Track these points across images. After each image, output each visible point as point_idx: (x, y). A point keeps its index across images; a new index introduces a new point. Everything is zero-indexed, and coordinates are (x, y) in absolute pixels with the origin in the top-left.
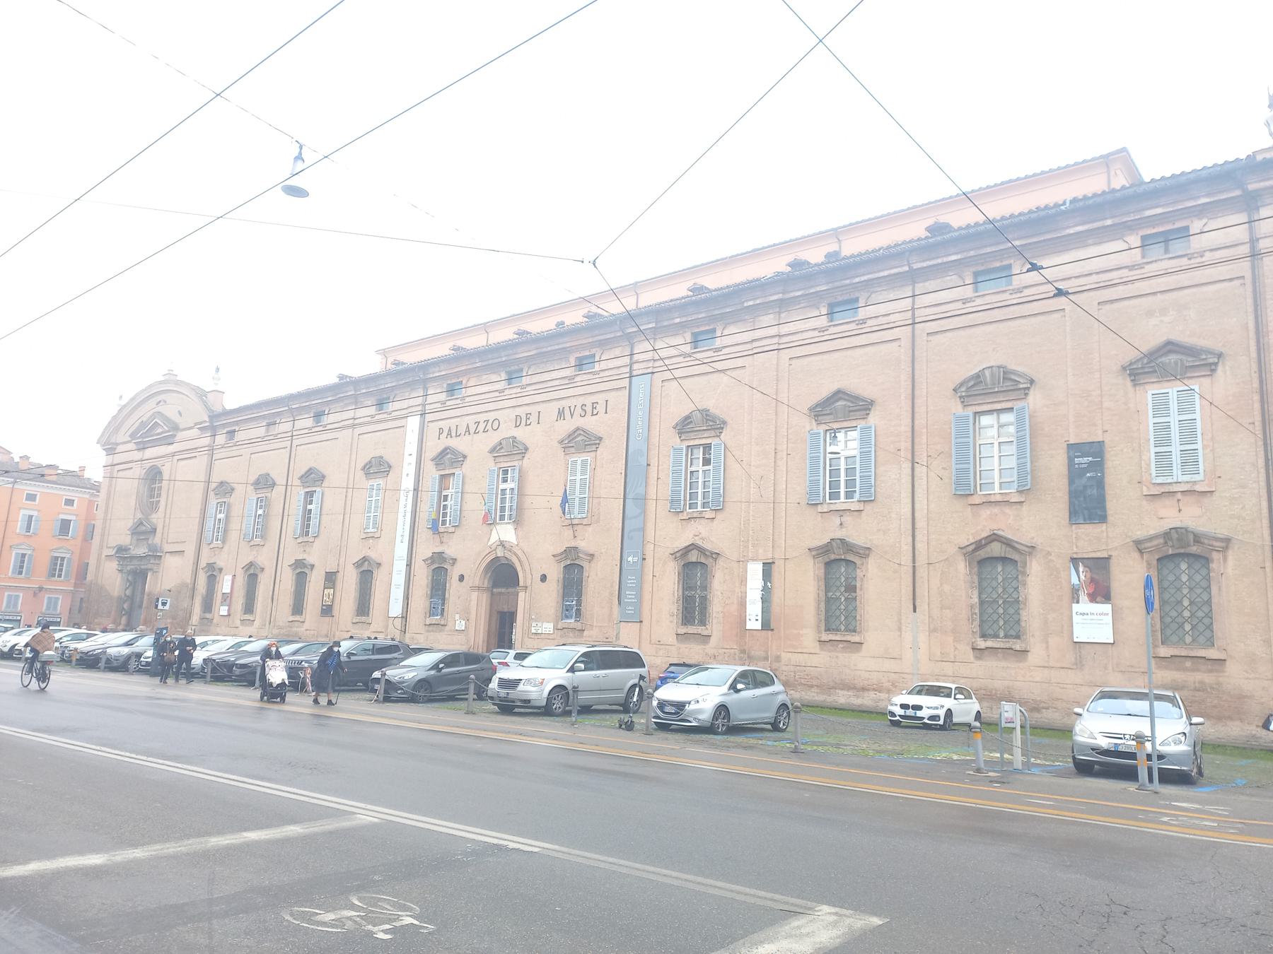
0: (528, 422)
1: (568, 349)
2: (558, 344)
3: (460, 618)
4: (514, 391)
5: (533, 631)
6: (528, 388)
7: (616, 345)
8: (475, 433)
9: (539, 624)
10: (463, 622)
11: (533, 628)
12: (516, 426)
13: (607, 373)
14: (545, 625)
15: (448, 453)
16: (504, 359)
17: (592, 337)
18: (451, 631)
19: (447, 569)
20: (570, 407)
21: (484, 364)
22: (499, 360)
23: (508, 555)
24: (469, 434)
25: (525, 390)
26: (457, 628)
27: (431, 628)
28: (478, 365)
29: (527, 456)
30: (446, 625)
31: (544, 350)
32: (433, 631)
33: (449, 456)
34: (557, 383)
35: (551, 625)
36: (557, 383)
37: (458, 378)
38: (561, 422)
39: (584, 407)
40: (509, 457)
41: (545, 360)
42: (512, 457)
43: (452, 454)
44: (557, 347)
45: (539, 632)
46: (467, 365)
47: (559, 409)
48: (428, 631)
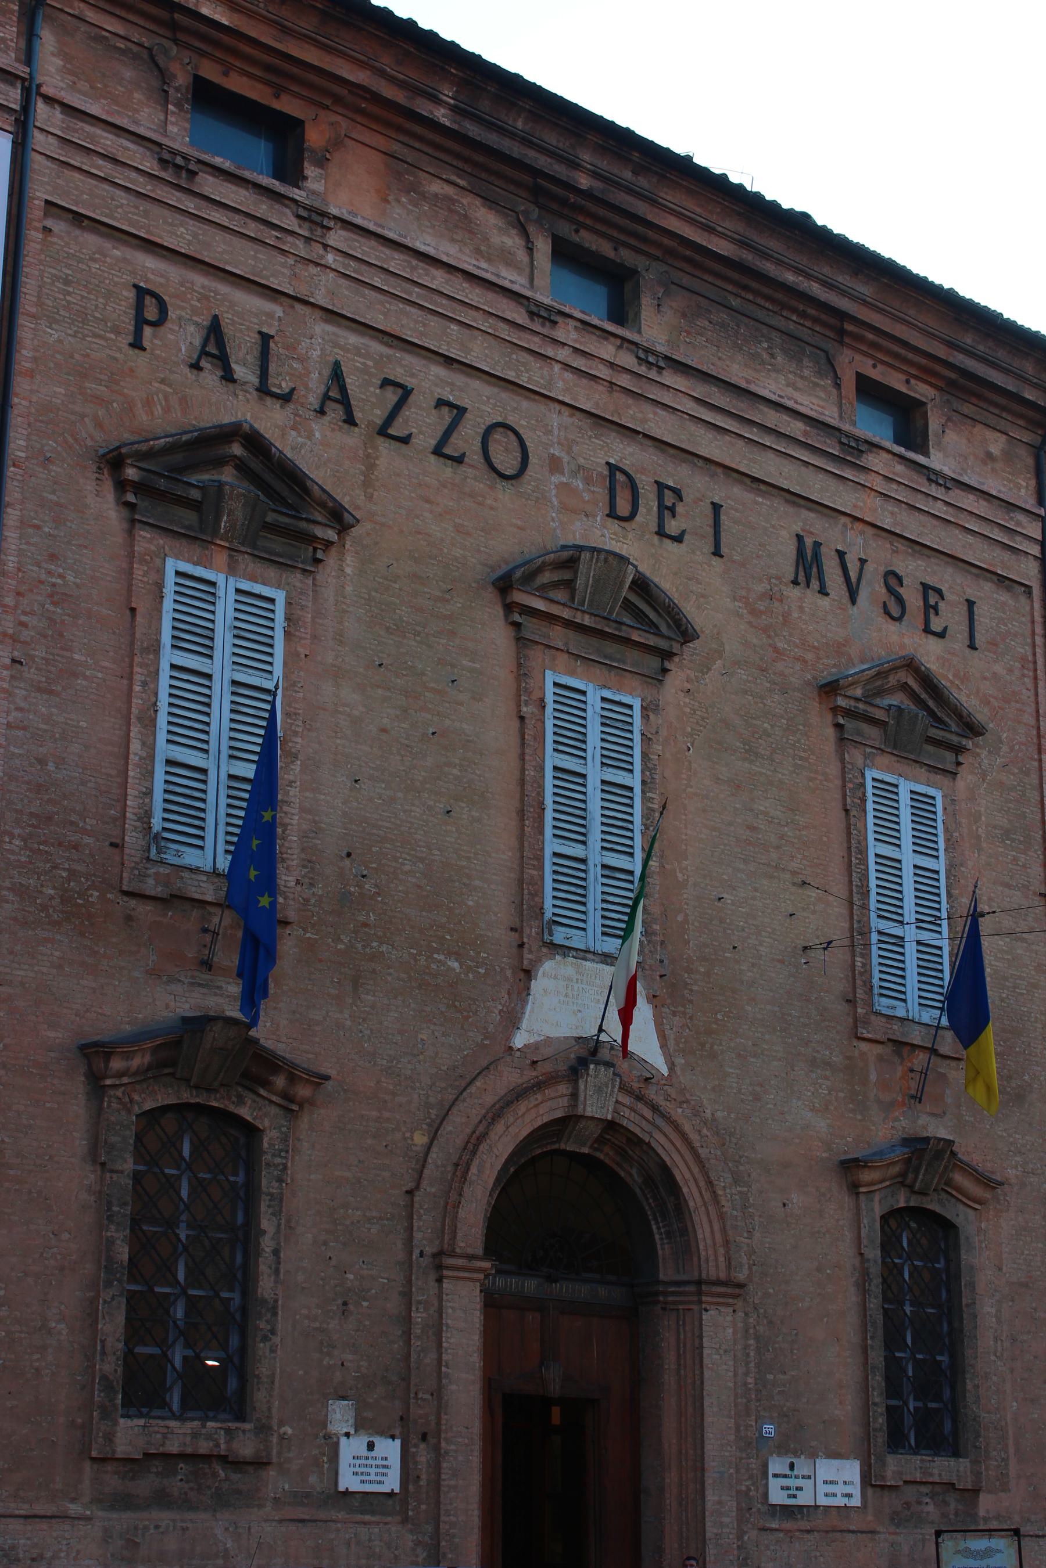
0: (673, 526)
1: (849, 327)
2: (826, 284)
3: (361, 1425)
4: (607, 350)
5: (777, 1496)
6: (669, 378)
7: (992, 420)
8: (383, 431)
9: (803, 1466)
10: (390, 1449)
11: (774, 1484)
12: (612, 514)
13: (969, 501)
14: (826, 1469)
15: (219, 463)
16: (584, 182)
17: (951, 345)
18: (302, 1498)
19: (252, 1131)
20: (841, 554)
21: (472, 130)
22: (560, 170)
23: (633, 1121)
24: (350, 421)
25: (653, 374)
26: (348, 1481)
27: (144, 1486)
28: (442, 115)
29: (677, 677)
30: (260, 1464)
31: (769, 268)
32: (162, 1499)
33: (228, 475)
34: (797, 428)
35: (851, 1471)
36: (797, 428)
37: (279, 91)
38: (811, 597)
39: (892, 582)
40: (594, 641)
41: (735, 302)
42: (611, 648)
43: (241, 467)
44: (816, 289)
45: (804, 1499)
46: (382, 73)
47: (799, 538)
48: (123, 1502)
